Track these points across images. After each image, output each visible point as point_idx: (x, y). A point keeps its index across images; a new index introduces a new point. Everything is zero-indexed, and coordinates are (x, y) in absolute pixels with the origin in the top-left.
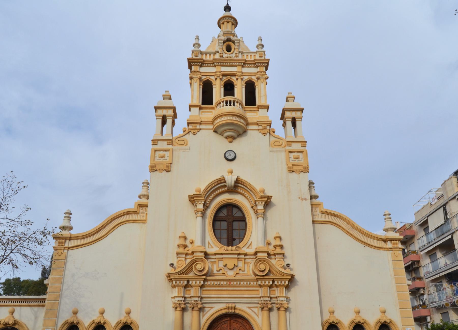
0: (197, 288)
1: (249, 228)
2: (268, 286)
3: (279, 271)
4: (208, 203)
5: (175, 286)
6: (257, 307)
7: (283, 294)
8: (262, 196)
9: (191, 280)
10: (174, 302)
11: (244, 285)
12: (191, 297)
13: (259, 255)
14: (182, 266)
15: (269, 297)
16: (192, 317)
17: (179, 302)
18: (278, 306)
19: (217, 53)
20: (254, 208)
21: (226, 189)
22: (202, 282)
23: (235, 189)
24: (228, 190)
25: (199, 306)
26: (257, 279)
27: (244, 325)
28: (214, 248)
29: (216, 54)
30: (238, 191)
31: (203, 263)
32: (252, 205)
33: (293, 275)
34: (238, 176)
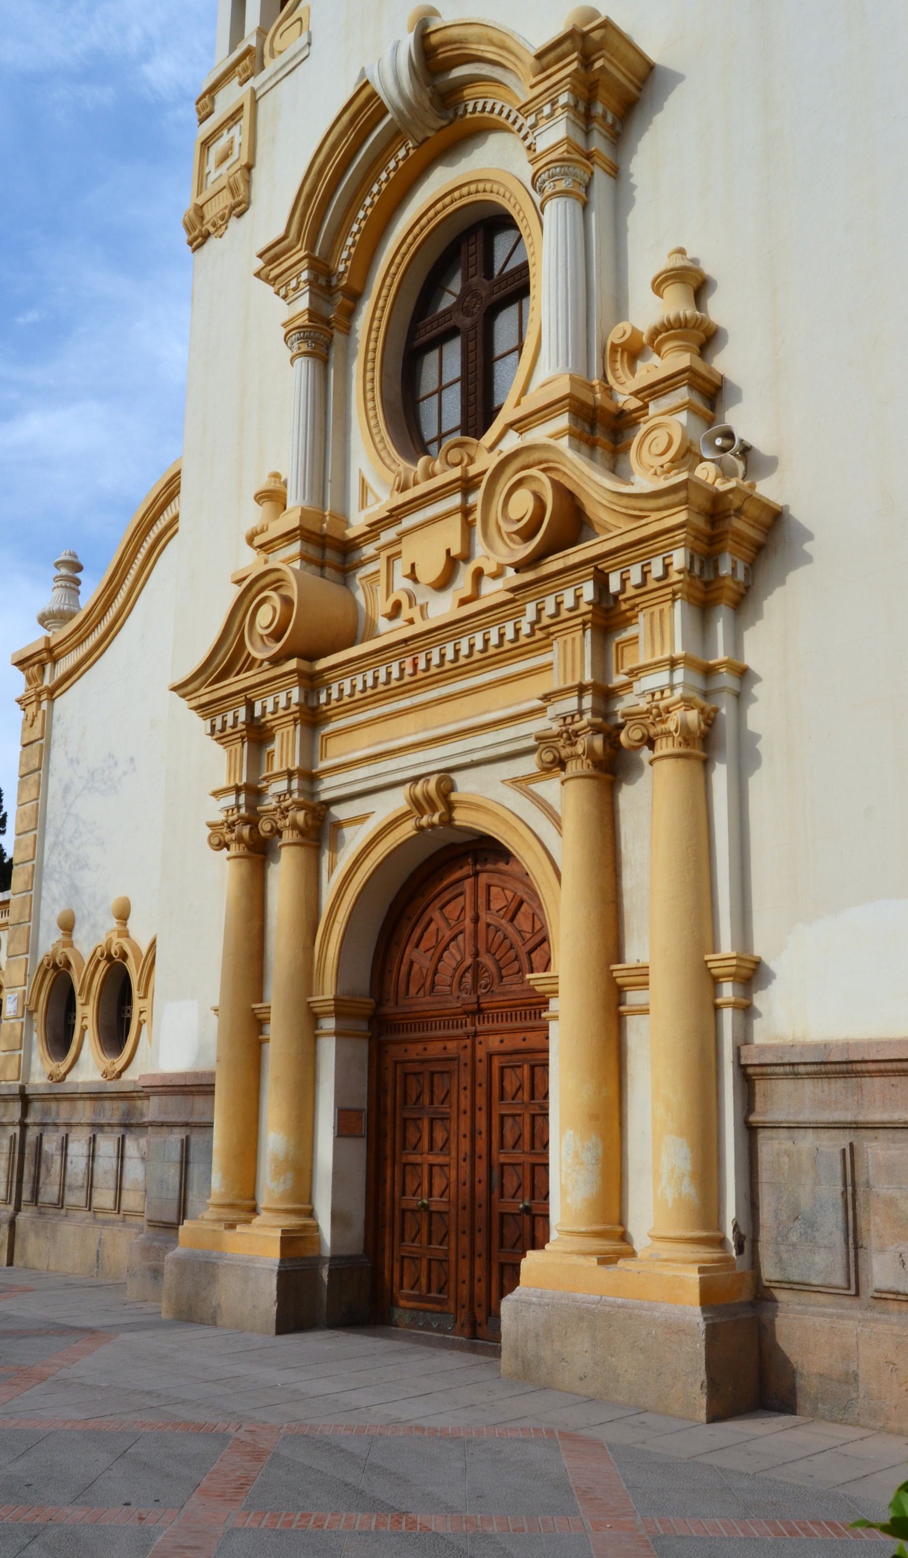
3: (615, 499)
8: (539, 56)
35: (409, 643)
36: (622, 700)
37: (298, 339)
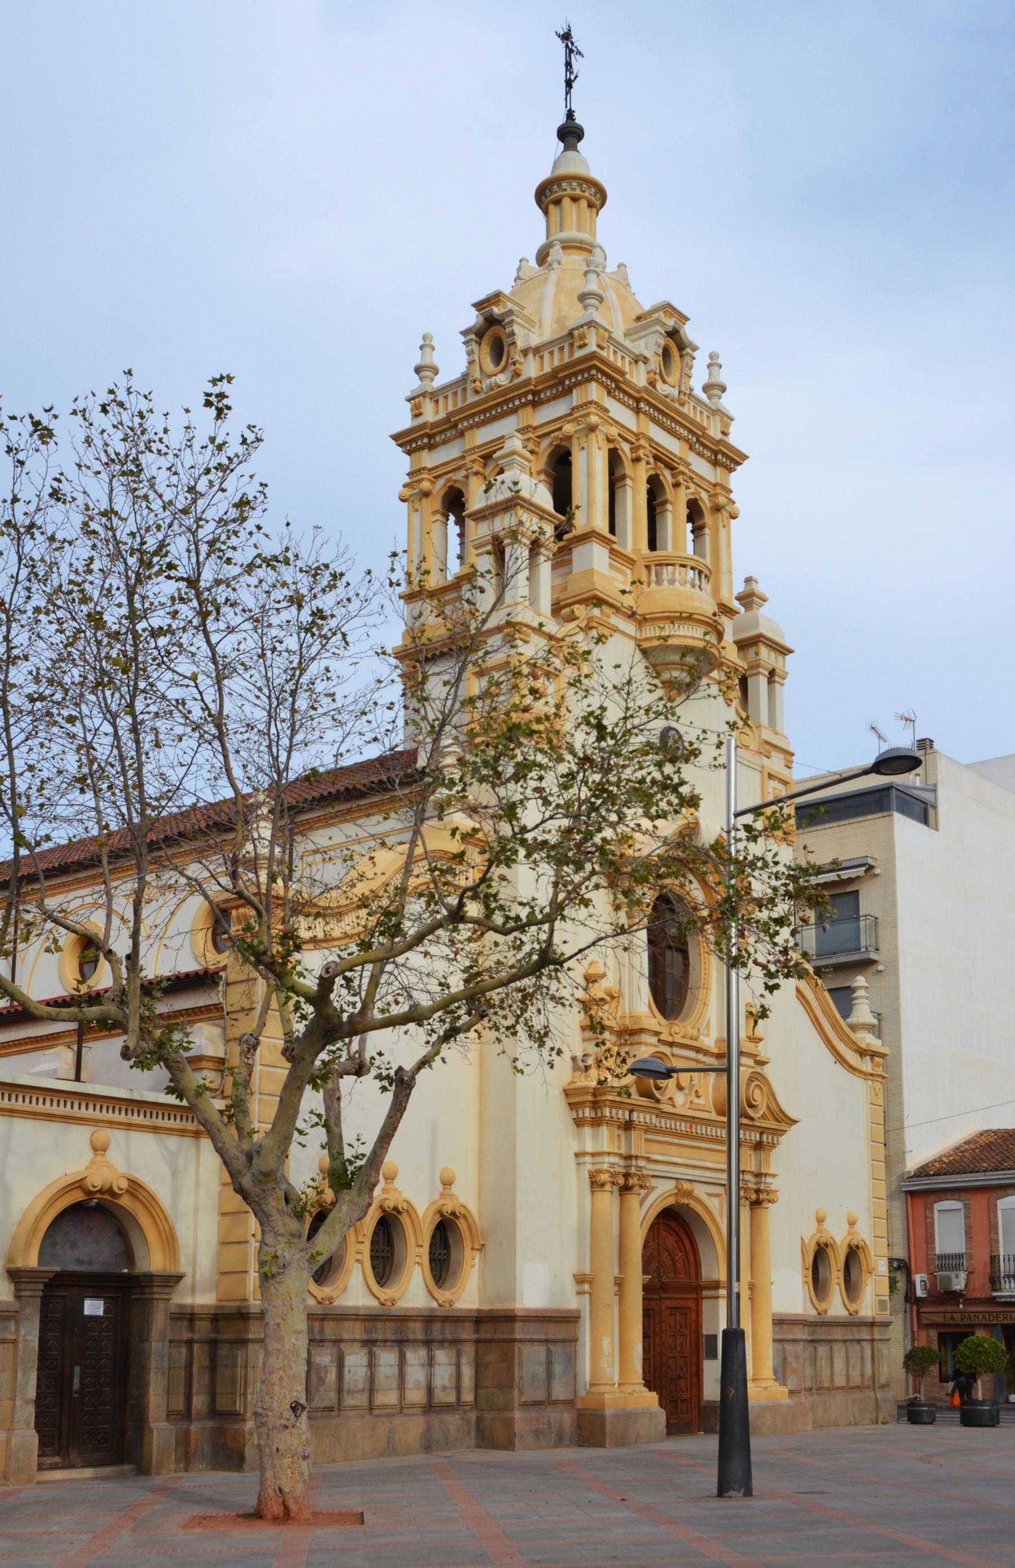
19: (641, 364)
29: (636, 362)
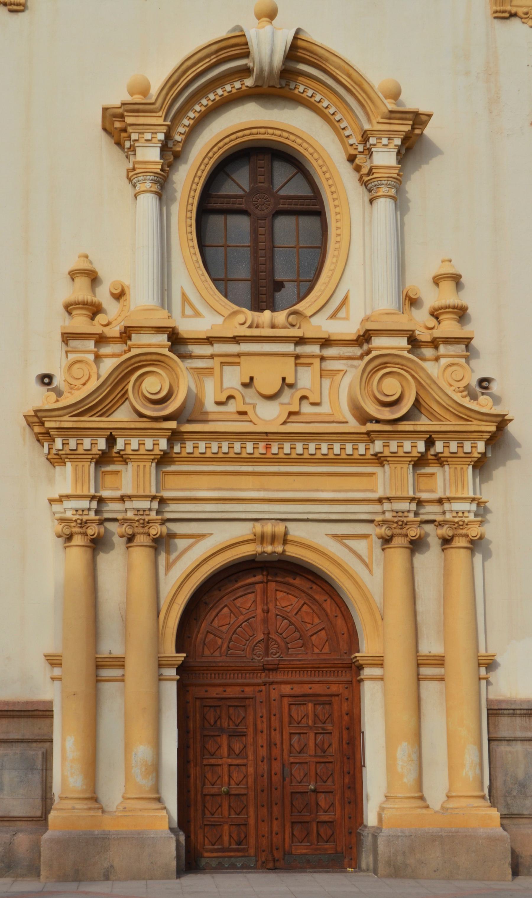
0: (145, 466)
1: (337, 242)
2: (409, 459)
3: (454, 405)
4: (178, 138)
5: (61, 459)
6: (365, 536)
7: (466, 489)
9: (121, 436)
10: (58, 516)
11: (319, 456)
12: (122, 499)
13: (377, 342)
14: (84, 384)
15: (413, 499)
16: (129, 568)
17: (80, 517)
18: (446, 531)
20: (357, 161)
21: (249, 82)
22: (163, 444)
23: (284, 83)
24: (258, 90)
25: (153, 532)
26: (368, 433)
27: (314, 599)
28: (204, 317)
30: (296, 92)
31: (166, 374)
32: (349, 147)
33: (506, 418)
34: (298, 31)
35: (269, 435)
36: (425, 508)
37: (152, 180)
